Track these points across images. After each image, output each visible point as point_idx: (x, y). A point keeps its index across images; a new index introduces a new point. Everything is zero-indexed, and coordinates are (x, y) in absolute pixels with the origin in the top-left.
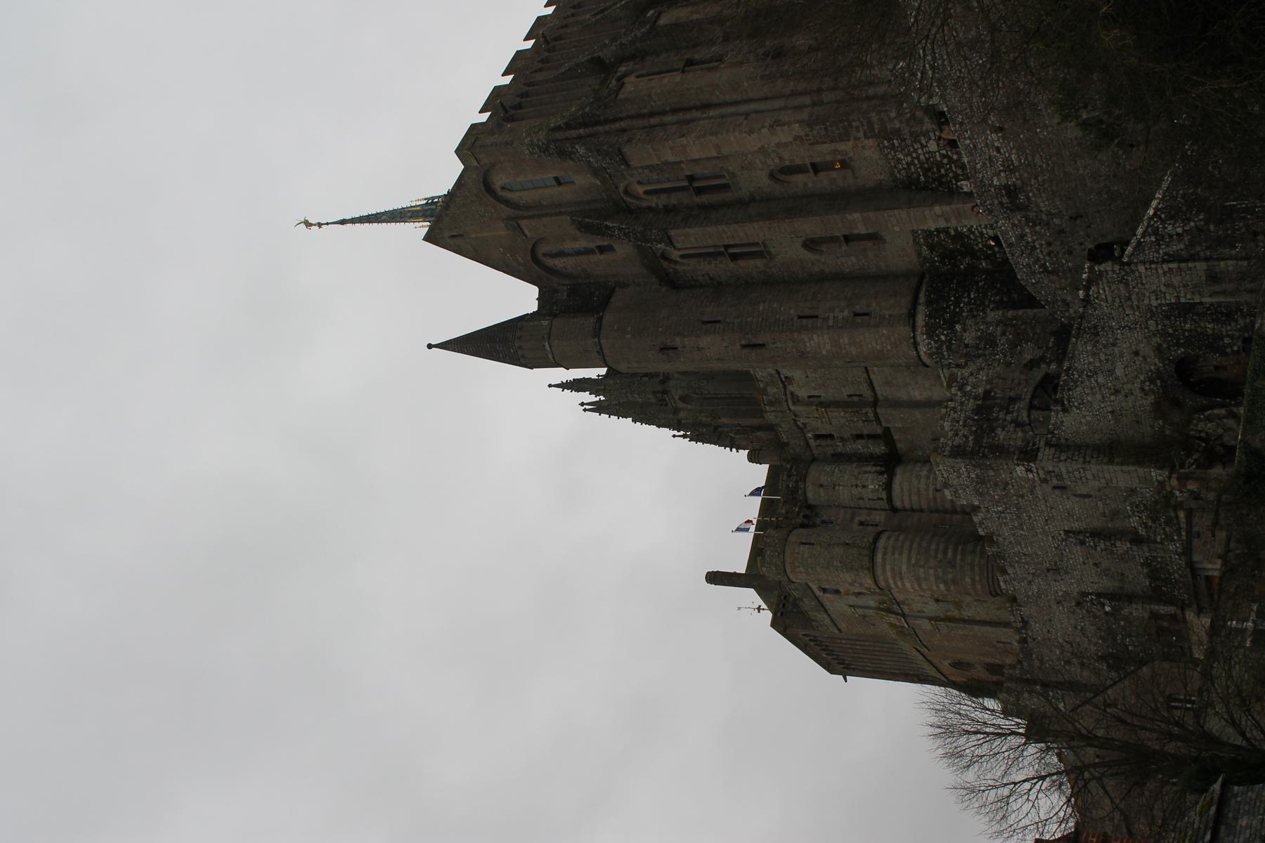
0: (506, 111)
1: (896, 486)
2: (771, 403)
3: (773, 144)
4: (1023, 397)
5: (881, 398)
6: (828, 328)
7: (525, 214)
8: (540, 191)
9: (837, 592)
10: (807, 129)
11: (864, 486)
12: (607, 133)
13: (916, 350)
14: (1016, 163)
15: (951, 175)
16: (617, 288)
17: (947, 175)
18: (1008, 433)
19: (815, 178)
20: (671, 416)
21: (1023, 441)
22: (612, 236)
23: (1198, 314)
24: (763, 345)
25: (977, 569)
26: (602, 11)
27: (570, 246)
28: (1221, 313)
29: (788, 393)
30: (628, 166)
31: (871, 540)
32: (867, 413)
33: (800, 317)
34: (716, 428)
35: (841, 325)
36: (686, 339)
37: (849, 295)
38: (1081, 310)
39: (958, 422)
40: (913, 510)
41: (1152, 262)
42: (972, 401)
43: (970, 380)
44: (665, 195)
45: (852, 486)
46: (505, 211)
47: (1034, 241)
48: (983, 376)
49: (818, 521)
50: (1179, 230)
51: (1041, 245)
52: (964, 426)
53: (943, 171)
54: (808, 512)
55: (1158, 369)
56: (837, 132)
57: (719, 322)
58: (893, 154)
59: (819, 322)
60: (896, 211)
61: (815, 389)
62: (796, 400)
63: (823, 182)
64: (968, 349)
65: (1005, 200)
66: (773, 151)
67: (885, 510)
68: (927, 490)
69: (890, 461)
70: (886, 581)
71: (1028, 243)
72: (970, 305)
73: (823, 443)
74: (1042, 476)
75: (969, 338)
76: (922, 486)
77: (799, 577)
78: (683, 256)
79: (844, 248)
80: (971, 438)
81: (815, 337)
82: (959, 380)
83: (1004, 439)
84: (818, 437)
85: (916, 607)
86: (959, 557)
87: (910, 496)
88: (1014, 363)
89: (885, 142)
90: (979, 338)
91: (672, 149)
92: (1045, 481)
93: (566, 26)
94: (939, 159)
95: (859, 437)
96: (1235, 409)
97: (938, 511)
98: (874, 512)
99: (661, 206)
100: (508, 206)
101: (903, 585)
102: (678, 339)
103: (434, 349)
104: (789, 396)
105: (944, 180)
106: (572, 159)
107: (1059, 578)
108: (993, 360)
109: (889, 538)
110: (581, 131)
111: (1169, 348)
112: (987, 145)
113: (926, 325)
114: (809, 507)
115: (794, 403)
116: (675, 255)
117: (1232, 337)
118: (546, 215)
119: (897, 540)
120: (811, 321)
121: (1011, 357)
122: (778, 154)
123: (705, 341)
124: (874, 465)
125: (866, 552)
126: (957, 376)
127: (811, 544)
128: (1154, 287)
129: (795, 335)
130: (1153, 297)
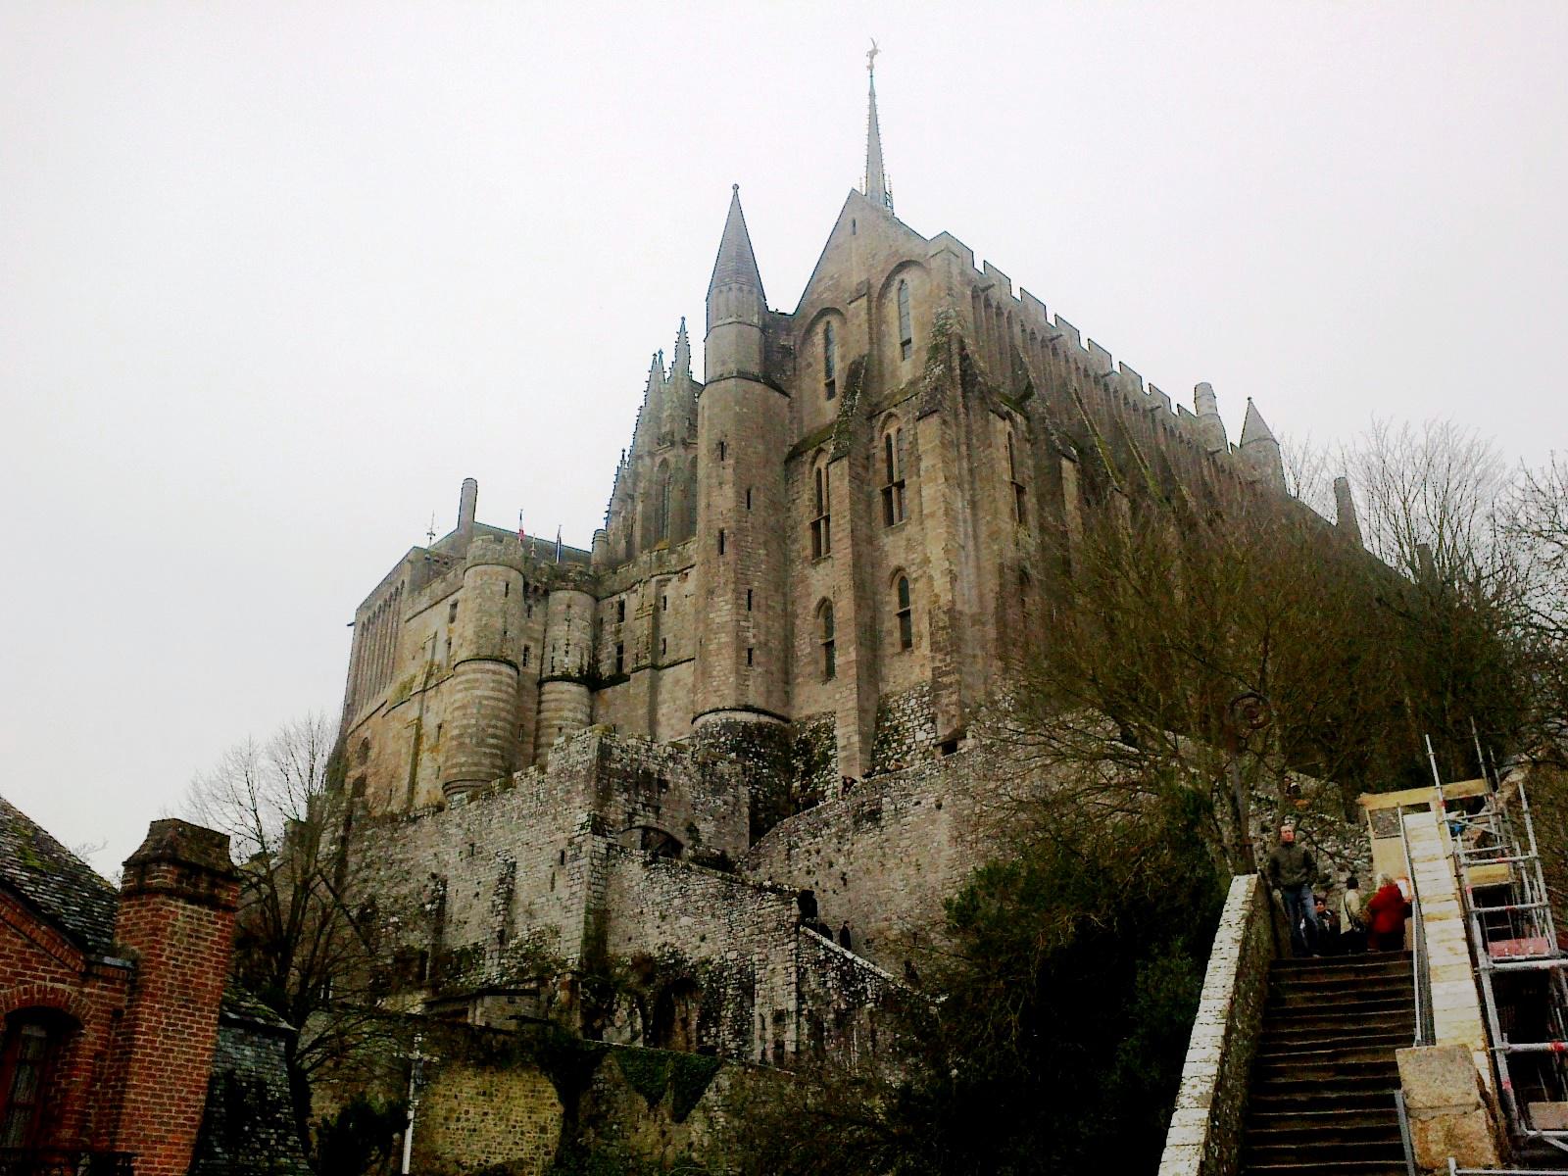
0: (983, 291)
1: (566, 686)
2: (659, 558)
3: (933, 573)
5: (661, 673)
7: (874, 304)
8: (897, 323)
9: (452, 619)
10: (945, 609)
11: (567, 652)
12: (954, 399)
14: (903, 821)
15: (890, 754)
16: (788, 399)
17: (890, 748)
20: (647, 449)
21: (613, 820)
22: (845, 397)
23: (741, 1002)
24: (722, 553)
25: (474, 769)
26: (1080, 401)
27: (836, 352)
28: (743, 1025)
29: (670, 576)
30: (919, 419)
33: (750, 591)
34: (632, 497)
36: (731, 470)
38: (751, 883)
39: (636, 753)
40: (540, 703)
41: (798, 956)
44: (885, 457)
46: (878, 283)
47: (822, 836)
48: (684, 779)
49: (531, 602)
50: (830, 984)
51: (817, 843)
52: (632, 760)
53: (894, 745)
54: (541, 591)
55: (686, 961)
57: (749, 507)
59: (744, 612)
60: (855, 696)
61: (673, 603)
63: (891, 624)
65: (866, 809)
66: (925, 572)
67: (541, 674)
68: (561, 718)
69: (592, 681)
70: (463, 673)
71: (821, 830)
73: (615, 610)
74: (576, 840)
75: (723, 767)
76: (566, 714)
77: (471, 579)
78: (819, 472)
79: (821, 641)
80: (619, 766)
81: (729, 606)
84: (622, 605)
85: (434, 704)
86: (488, 751)
87: (556, 700)
90: (722, 777)
91: (933, 466)
92: (571, 843)
93: (1067, 361)
94: (907, 742)
95: (620, 649)
96: (641, 1038)
97: (537, 729)
98: (539, 662)
99: (875, 451)
100: (883, 285)
101: (460, 691)
102: (732, 462)
103: (732, 191)
104: (667, 576)
105: (885, 746)
106: (929, 359)
107: (464, 856)
109: (511, 677)
110: (958, 371)
111: (707, 972)
112: (923, 792)
114: (546, 593)
115: (659, 581)
116: (822, 463)
117: (717, 1036)
118: (870, 328)
119: (509, 685)
120: (745, 603)
123: (729, 491)
125: (497, 653)
127: (506, 594)
128: (772, 958)
129: (732, 586)
130: (762, 957)
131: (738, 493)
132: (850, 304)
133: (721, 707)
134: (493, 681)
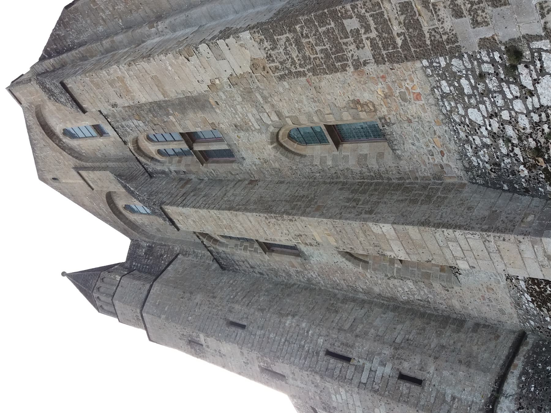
10: (267, 44)
19: (336, 153)
37: (398, 340)
56: (318, 48)
57: (243, 327)
58: (462, 112)
60: (458, 233)
89: (444, 83)
91: (112, 83)
120: (340, 364)
122: (273, 106)
129: (318, 378)
131: (227, 338)
132: (93, 189)
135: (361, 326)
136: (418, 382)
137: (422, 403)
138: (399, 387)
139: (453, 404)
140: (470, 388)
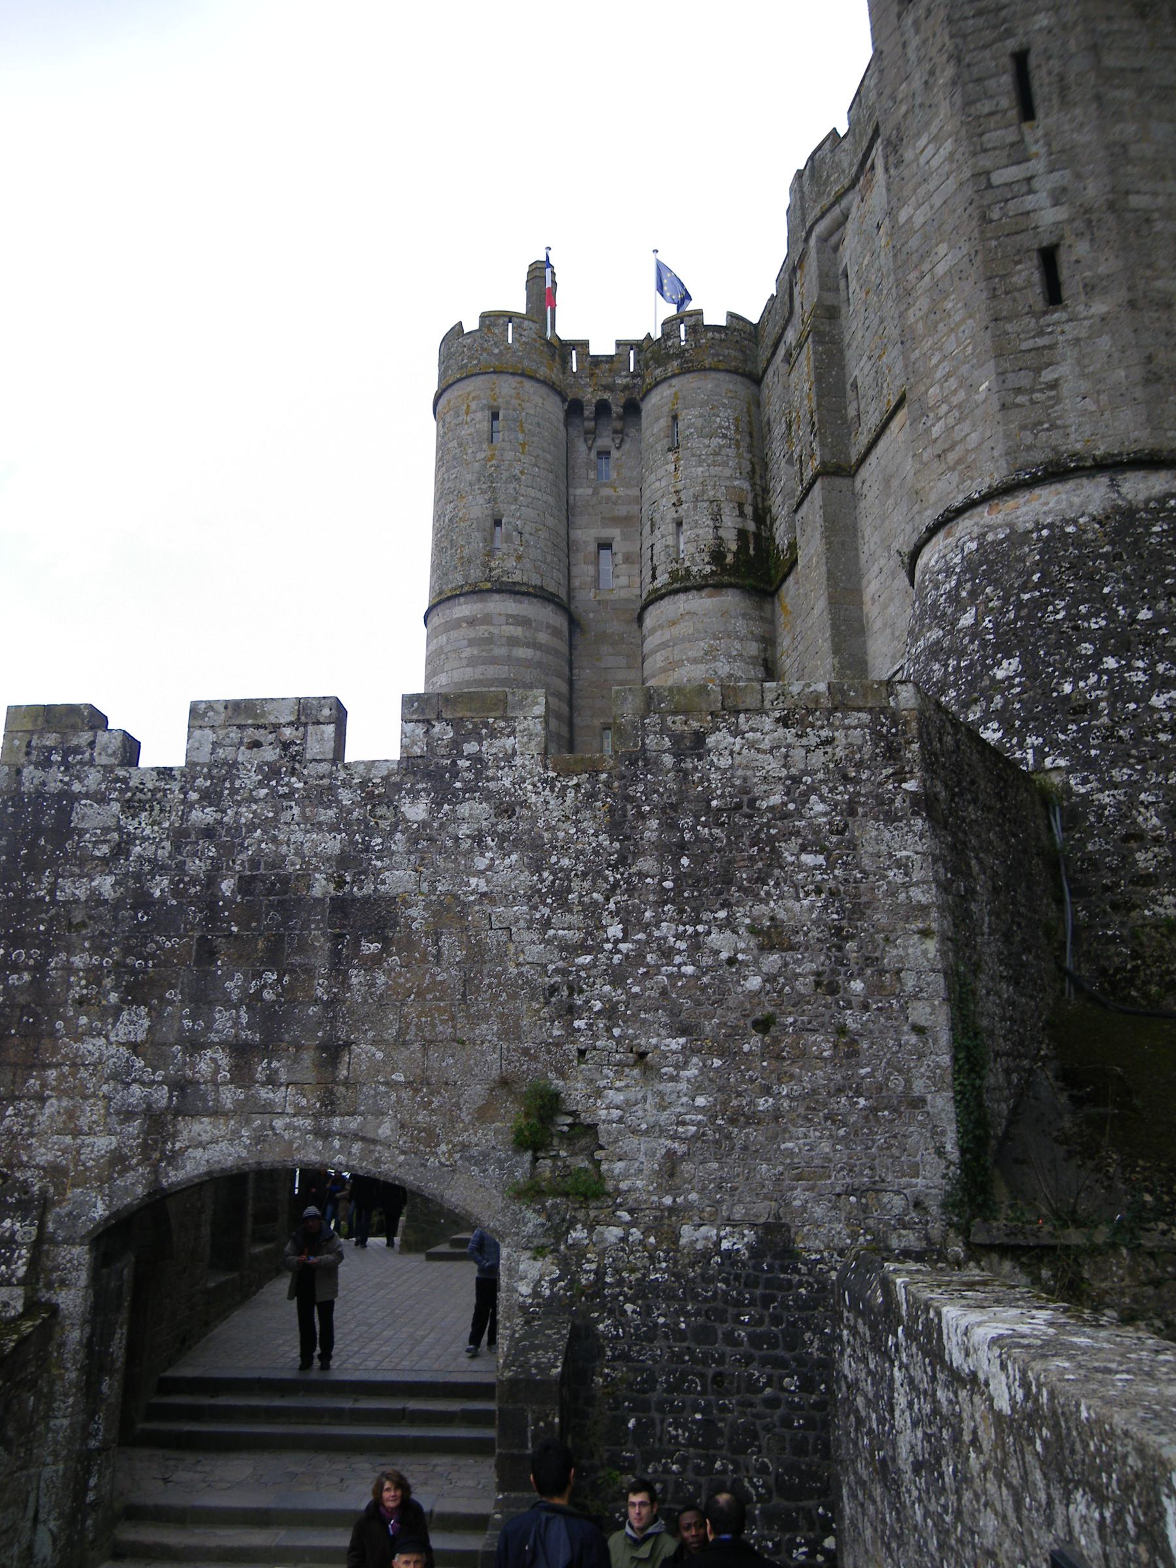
4: (336, 1122)
6: (982, 176)
13: (932, 531)
18: (115, 1076)
21: (55, 1171)
29: (844, 203)
31: (517, 577)
32: (812, 456)
33: (1021, 59)
35: (995, 215)
37: (1134, 201)
42: (333, 844)
43: (464, 809)
45: (677, 492)
49: (604, 442)
54: (616, 410)
62: (834, 240)
64: (668, 760)
72: (1116, 697)
82: (470, 748)
83: (76, 1064)
88: (572, 1032)
108: (592, 911)
109: (524, 622)
113: (1017, 538)
114: (633, 409)
115: (824, 239)
120: (1007, 101)
121: (611, 1012)
124: (742, 534)
125: (475, 573)
126: (494, 734)
133: (957, 503)
134: (471, 643)
135: (1128, 94)
136: (1054, 295)
137: (1009, 327)
138: (1017, 263)
139: (1041, 391)
140: (1093, 408)
